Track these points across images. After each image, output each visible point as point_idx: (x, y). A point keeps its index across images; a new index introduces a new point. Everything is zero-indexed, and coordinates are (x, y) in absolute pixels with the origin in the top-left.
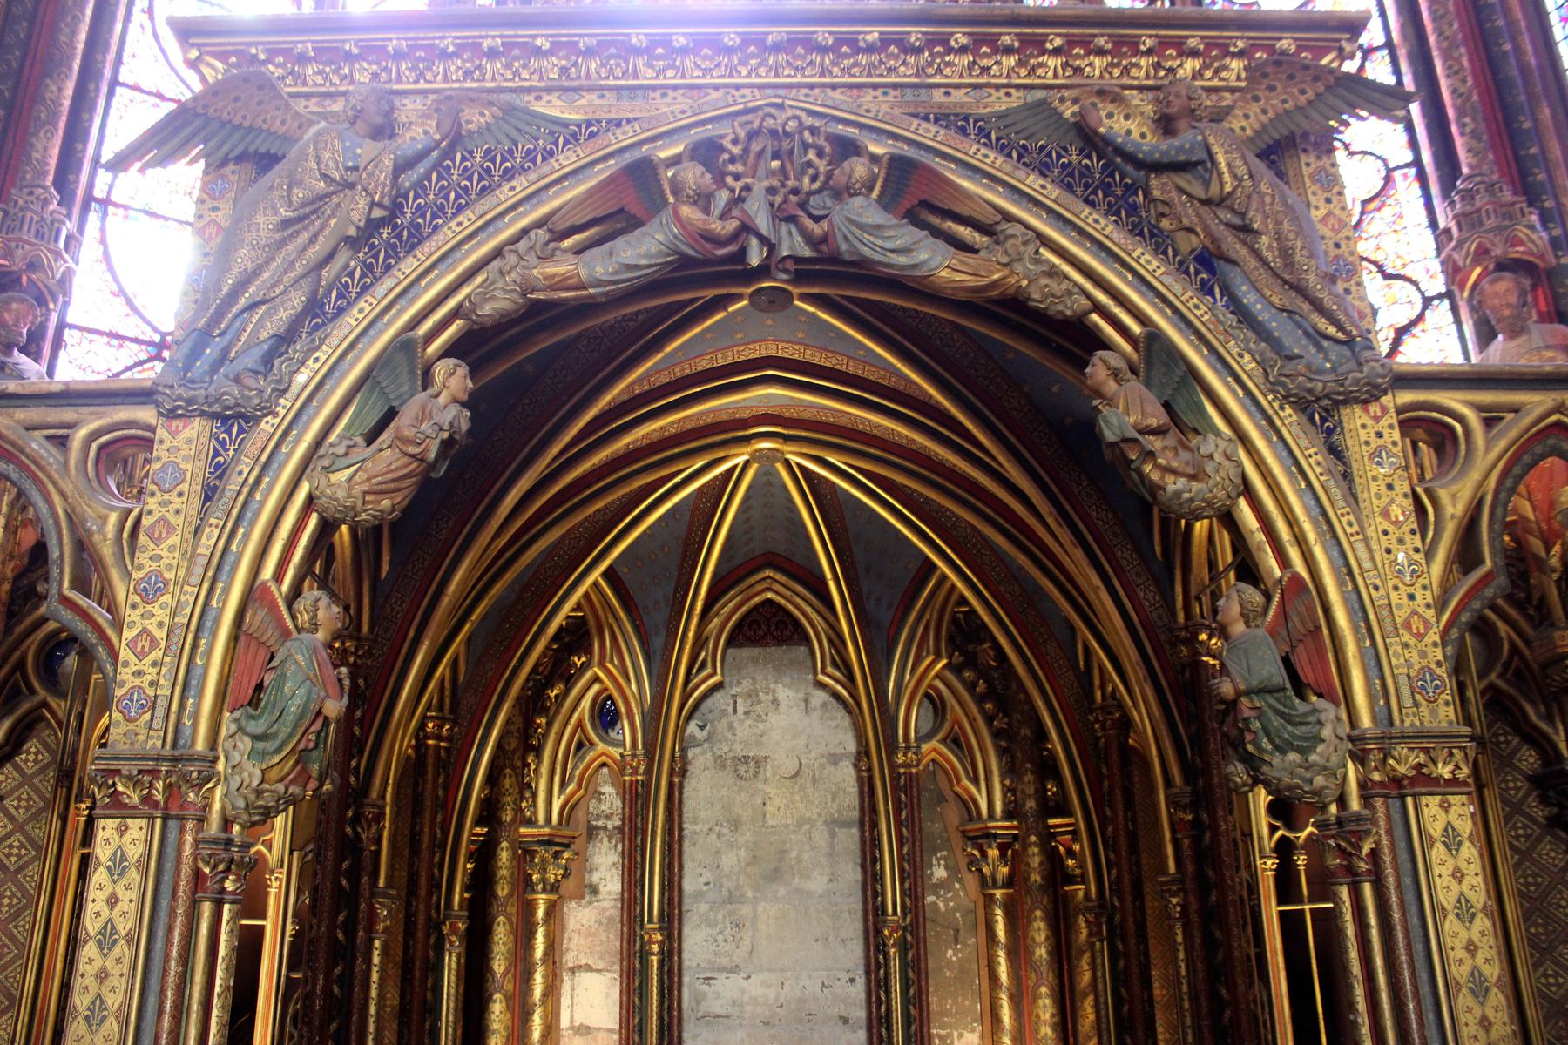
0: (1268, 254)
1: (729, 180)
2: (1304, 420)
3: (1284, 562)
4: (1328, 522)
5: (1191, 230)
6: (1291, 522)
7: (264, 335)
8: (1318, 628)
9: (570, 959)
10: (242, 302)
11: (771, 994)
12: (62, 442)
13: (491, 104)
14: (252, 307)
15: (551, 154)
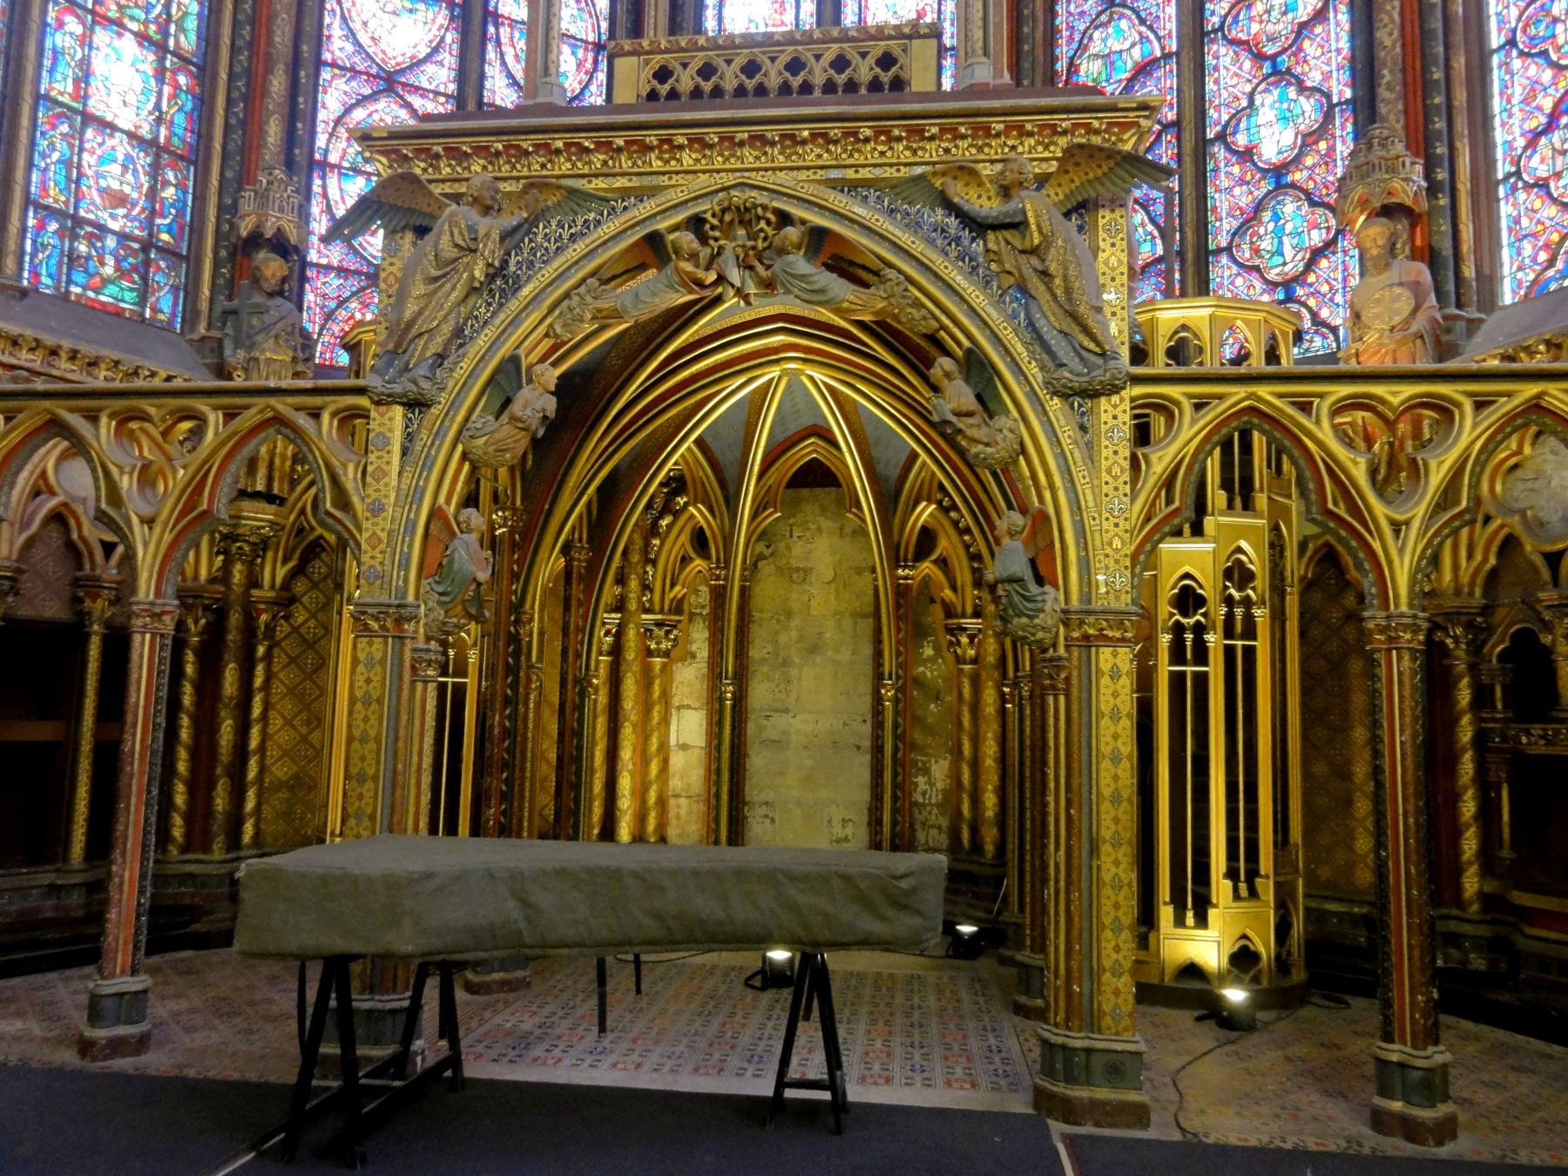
0: (1059, 292)
1: (712, 242)
2: (1067, 407)
3: (1041, 499)
4: (1070, 474)
5: (1009, 273)
6: (1048, 475)
7: (429, 354)
8: (1052, 543)
9: (676, 702)
10: (414, 332)
11: (809, 728)
12: (315, 415)
13: (559, 187)
14: (421, 335)
15: (599, 222)
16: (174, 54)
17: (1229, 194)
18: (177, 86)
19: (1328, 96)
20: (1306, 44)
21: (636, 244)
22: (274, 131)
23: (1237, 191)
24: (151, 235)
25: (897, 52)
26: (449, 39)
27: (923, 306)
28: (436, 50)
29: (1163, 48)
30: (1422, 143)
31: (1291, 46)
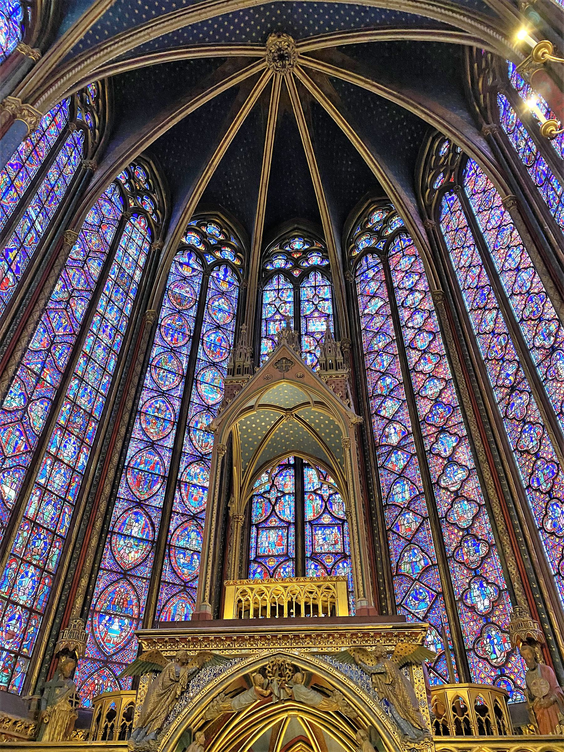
13: (211, 654)
14: (153, 720)
16: (46, 571)
17: (470, 627)
18: (45, 584)
19: (499, 587)
20: (486, 565)
21: (240, 678)
22: (79, 602)
23: (472, 624)
24: (20, 650)
25: (332, 587)
26: (150, 556)
27: (350, 706)
28: (144, 560)
29: (432, 562)
30: (535, 614)
31: (480, 566)
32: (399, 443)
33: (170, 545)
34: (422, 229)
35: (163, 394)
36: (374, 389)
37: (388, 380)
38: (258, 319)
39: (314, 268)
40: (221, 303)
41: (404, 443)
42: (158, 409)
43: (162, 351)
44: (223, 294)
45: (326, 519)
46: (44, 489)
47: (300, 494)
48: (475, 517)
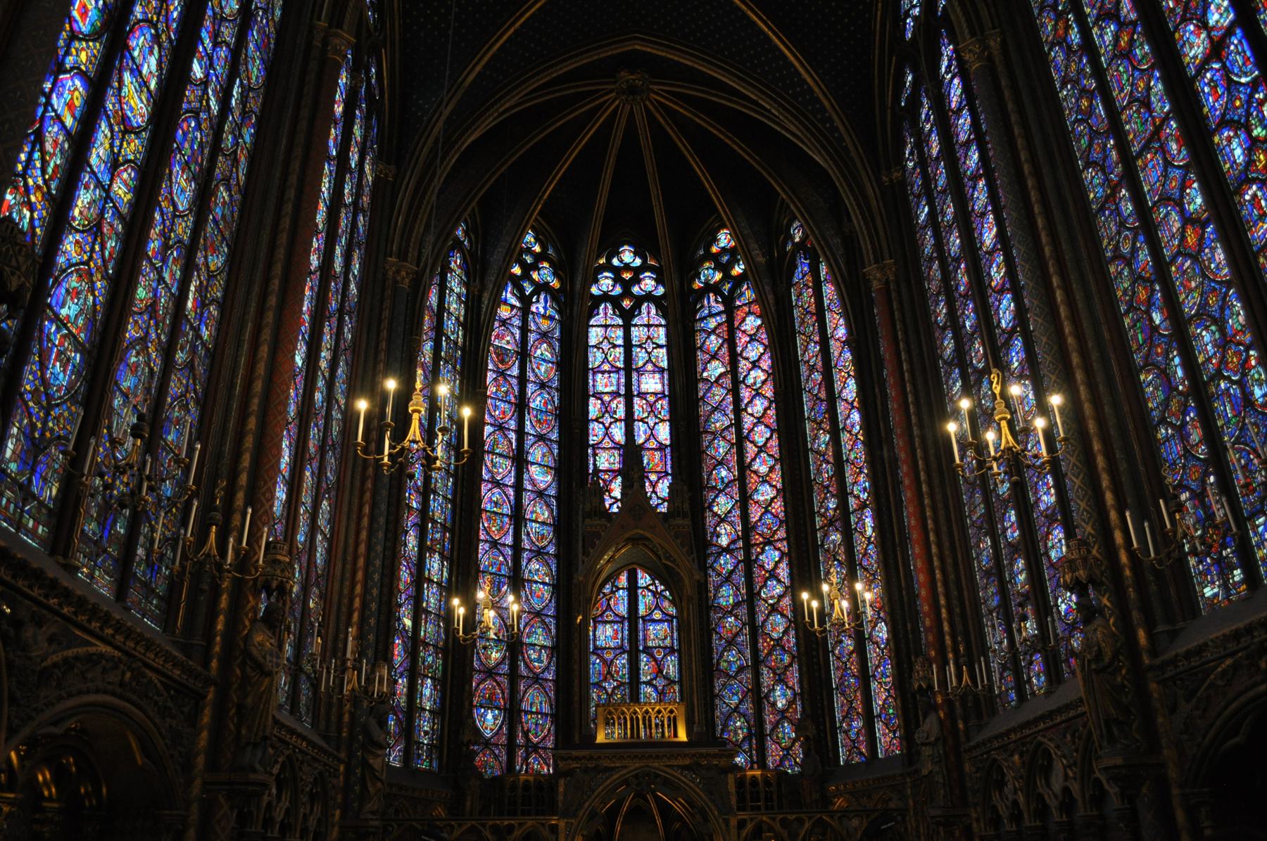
17: (769, 718)
32: (729, 545)
33: (522, 643)
34: (771, 297)
35: (497, 484)
36: (709, 479)
37: (724, 473)
38: (586, 369)
39: (649, 297)
40: (543, 351)
41: (732, 546)
42: (496, 503)
43: (491, 429)
44: (544, 336)
45: (657, 615)
46: (428, 613)
47: (633, 589)
48: (786, 632)
